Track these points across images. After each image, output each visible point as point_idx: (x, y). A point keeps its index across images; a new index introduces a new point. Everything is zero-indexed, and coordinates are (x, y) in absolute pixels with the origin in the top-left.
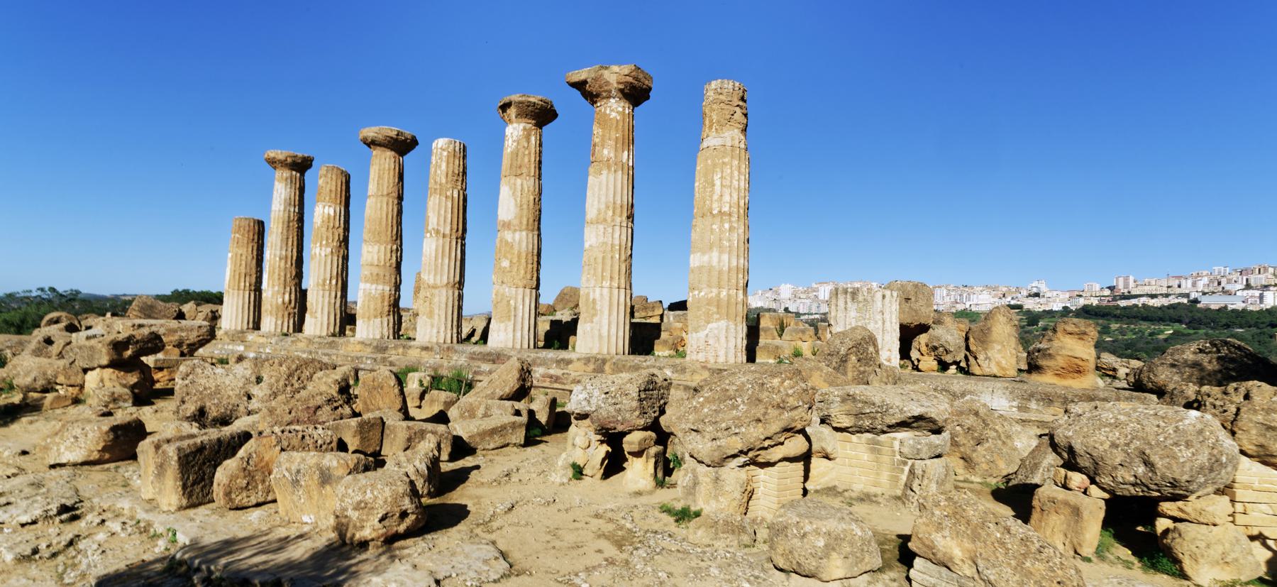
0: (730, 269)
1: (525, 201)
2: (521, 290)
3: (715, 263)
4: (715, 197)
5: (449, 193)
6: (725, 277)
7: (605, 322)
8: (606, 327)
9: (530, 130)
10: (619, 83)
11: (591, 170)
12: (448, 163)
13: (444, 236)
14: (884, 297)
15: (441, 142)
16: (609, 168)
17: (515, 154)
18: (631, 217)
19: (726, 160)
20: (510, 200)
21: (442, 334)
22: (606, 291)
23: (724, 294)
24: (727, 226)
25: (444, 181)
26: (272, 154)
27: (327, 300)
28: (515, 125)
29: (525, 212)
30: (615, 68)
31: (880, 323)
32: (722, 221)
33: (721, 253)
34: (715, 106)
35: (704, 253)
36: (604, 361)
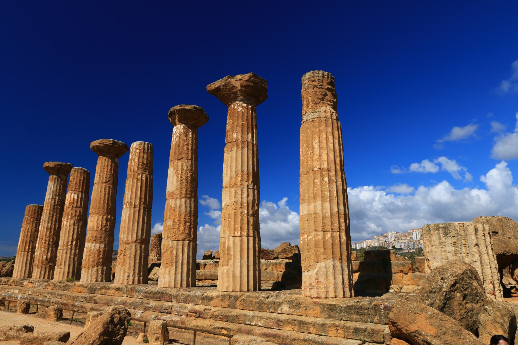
0: (332, 215)
1: (184, 176)
2: (181, 242)
4: (316, 157)
5: (139, 177)
6: (329, 222)
7: (238, 264)
8: (238, 269)
10: (242, 86)
11: (226, 149)
12: (139, 157)
13: (135, 207)
14: (476, 230)
15: (135, 145)
16: (237, 146)
17: (178, 145)
18: (256, 181)
19: (322, 128)
20: (174, 179)
21: (131, 278)
22: (238, 240)
23: (329, 235)
24: (326, 179)
25: (136, 169)
26: (46, 164)
27: (68, 255)
28: (178, 126)
29: (184, 184)
30: (239, 77)
31: (477, 255)
32: (322, 177)
33: (323, 202)
34: (310, 90)
35: (309, 203)
36: (236, 298)
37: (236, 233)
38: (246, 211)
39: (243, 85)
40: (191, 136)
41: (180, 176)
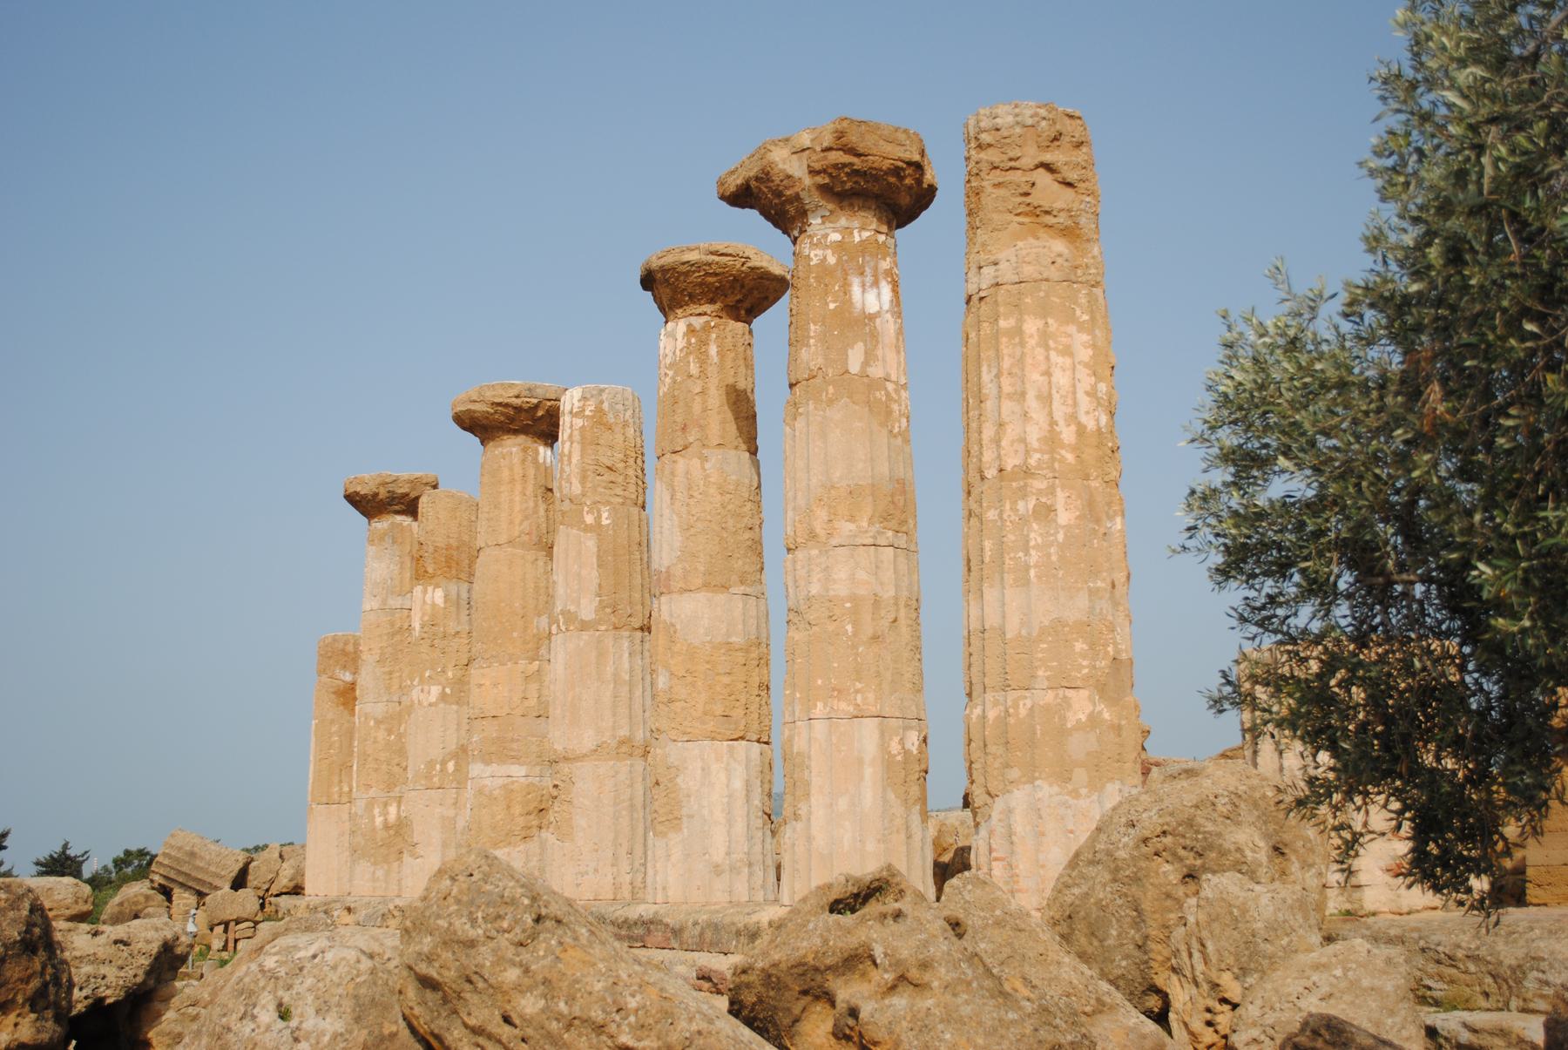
3: (992, 620)
9: (706, 328)
10: (813, 172)
25: (577, 488)
37: (820, 705)
38: (849, 628)
39: (817, 166)
40: (716, 360)
41: (684, 509)
